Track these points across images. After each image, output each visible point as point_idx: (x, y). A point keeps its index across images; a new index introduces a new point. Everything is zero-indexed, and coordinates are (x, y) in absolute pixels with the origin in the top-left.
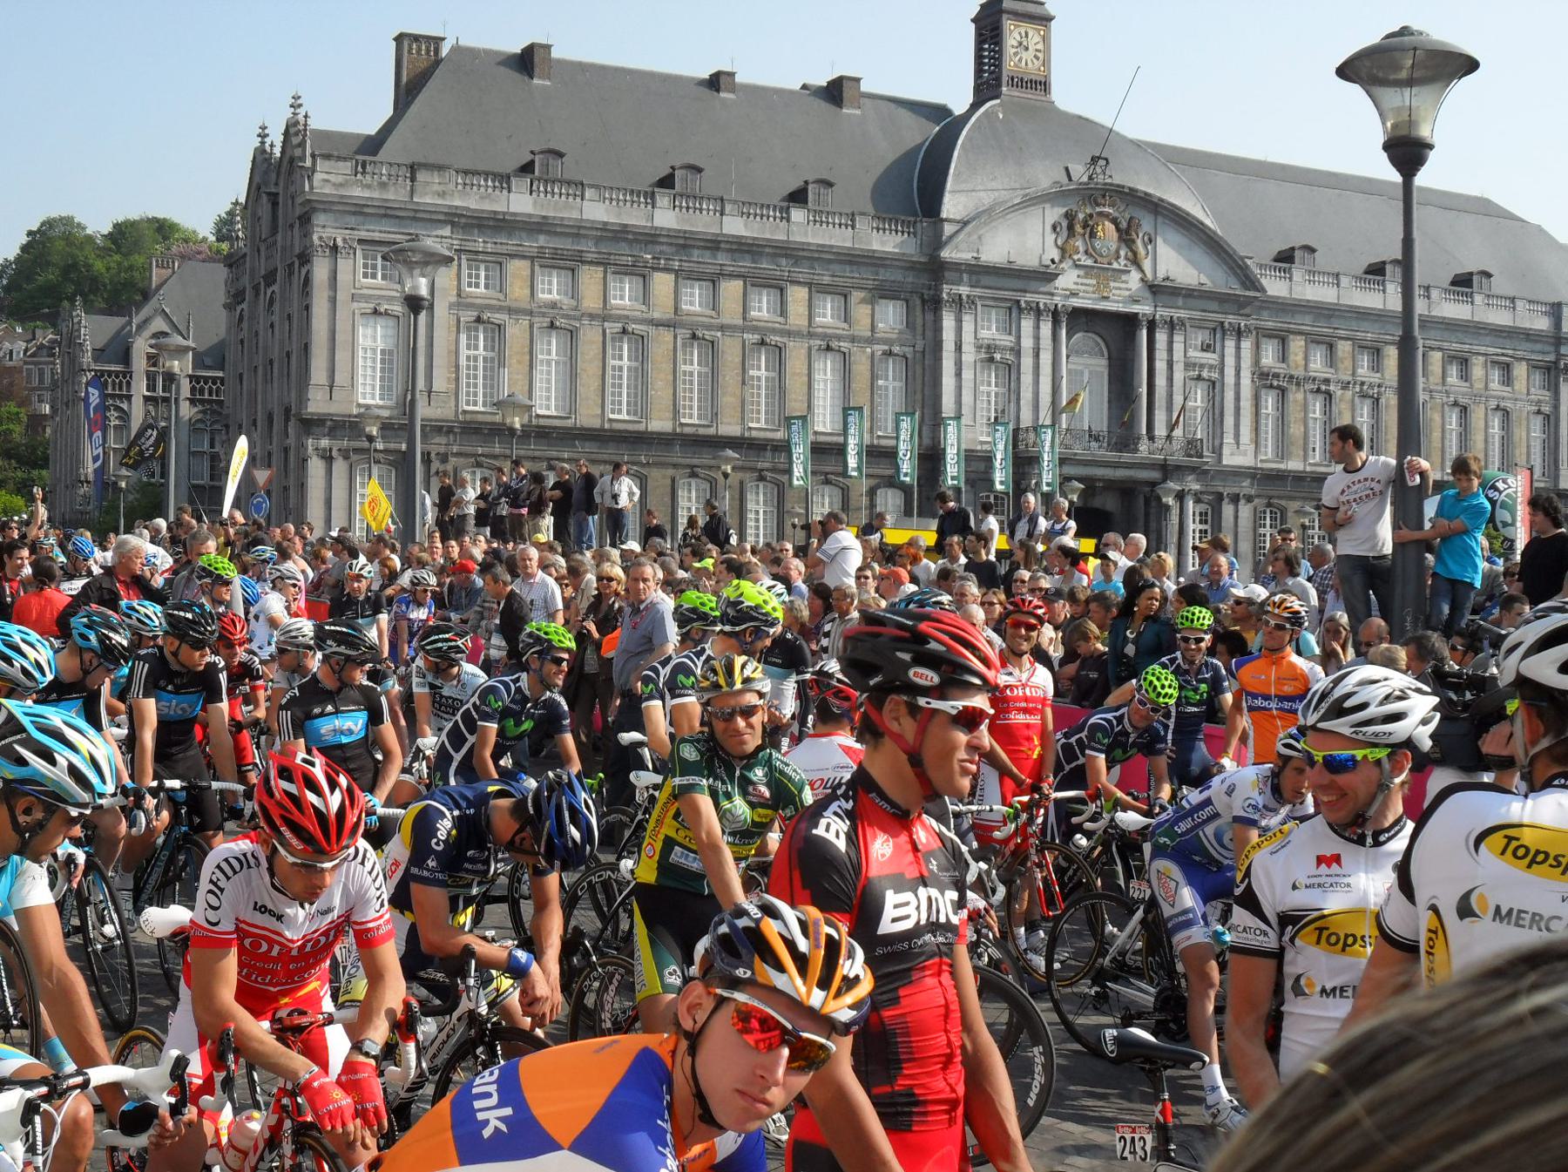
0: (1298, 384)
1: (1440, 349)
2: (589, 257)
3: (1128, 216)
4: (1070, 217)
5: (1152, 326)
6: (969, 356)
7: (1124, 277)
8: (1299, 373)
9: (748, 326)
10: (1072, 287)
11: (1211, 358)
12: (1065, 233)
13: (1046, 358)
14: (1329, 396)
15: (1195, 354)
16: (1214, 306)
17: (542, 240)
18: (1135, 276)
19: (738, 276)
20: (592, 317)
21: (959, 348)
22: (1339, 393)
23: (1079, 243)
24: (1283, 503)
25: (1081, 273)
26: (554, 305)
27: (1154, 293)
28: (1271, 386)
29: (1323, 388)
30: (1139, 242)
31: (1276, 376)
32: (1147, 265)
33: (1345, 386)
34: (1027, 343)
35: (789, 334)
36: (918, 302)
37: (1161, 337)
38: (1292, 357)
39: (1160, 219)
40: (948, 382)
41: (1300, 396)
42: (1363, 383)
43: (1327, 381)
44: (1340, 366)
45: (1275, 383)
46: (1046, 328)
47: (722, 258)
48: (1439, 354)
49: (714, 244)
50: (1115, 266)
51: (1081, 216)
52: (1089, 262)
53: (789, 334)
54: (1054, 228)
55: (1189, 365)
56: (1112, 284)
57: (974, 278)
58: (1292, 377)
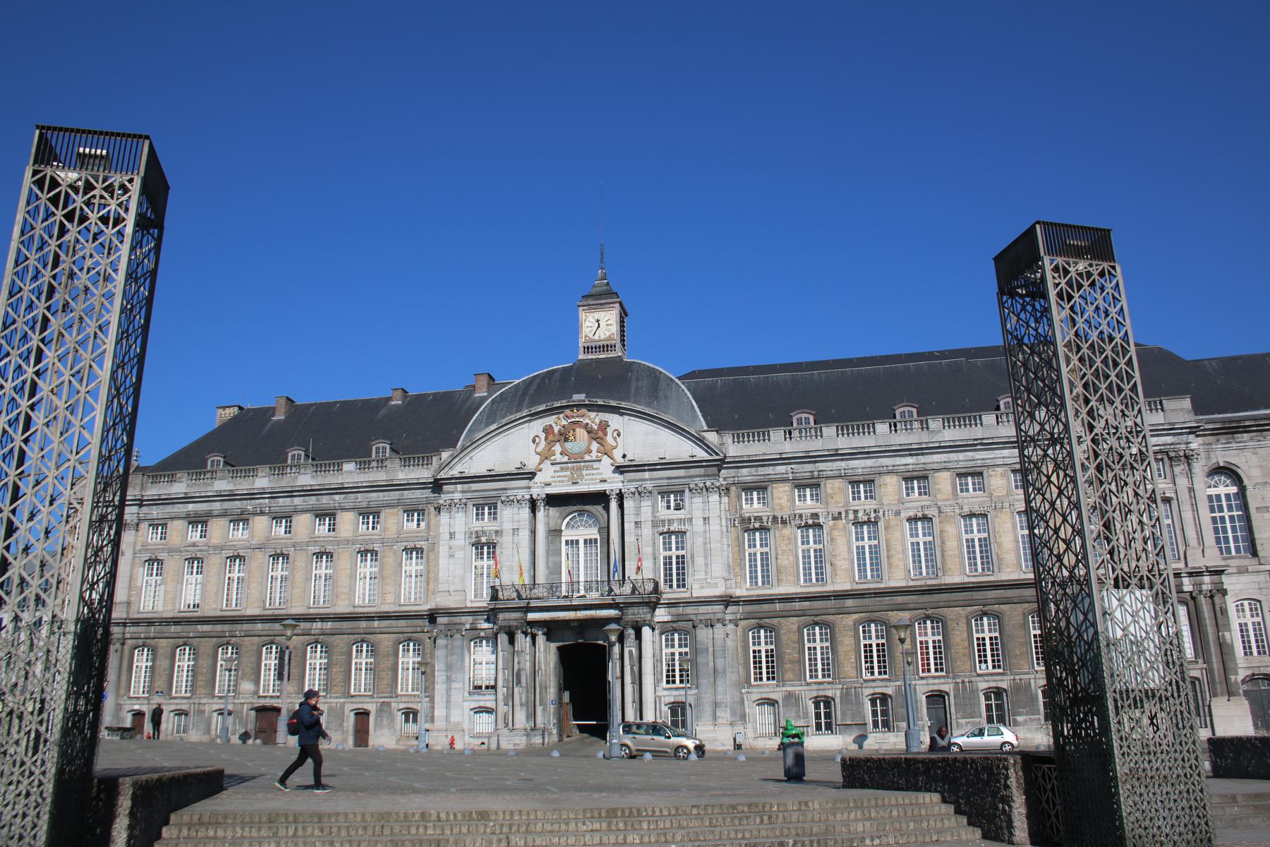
0: (784, 522)
1: (949, 469)
2: (215, 513)
3: (597, 421)
4: (548, 430)
5: (621, 496)
6: (460, 540)
7: (596, 465)
8: (785, 514)
9: (314, 541)
10: (552, 480)
11: (681, 514)
12: (543, 443)
13: (525, 534)
14: (820, 526)
15: (663, 513)
16: (681, 473)
17: (191, 507)
18: (606, 459)
19: (307, 511)
20: (215, 548)
21: (452, 535)
22: (831, 523)
23: (557, 448)
24: (775, 621)
25: (557, 467)
26: (194, 545)
27: (622, 473)
28: (755, 530)
29: (810, 522)
30: (609, 439)
31: (758, 519)
32: (617, 454)
33: (837, 517)
34: (507, 526)
35: (338, 543)
36: (432, 509)
37: (628, 504)
38: (776, 501)
39: (626, 417)
40: (443, 560)
41: (787, 531)
42: (856, 512)
43: (815, 516)
44: (830, 500)
45: (757, 525)
46: (526, 512)
47: (297, 501)
48: (946, 475)
49: (290, 494)
50: (587, 458)
51: (556, 429)
52: (565, 459)
53: (338, 543)
54: (534, 441)
55: (655, 524)
56: (584, 472)
57: (466, 486)
58: (775, 518)
